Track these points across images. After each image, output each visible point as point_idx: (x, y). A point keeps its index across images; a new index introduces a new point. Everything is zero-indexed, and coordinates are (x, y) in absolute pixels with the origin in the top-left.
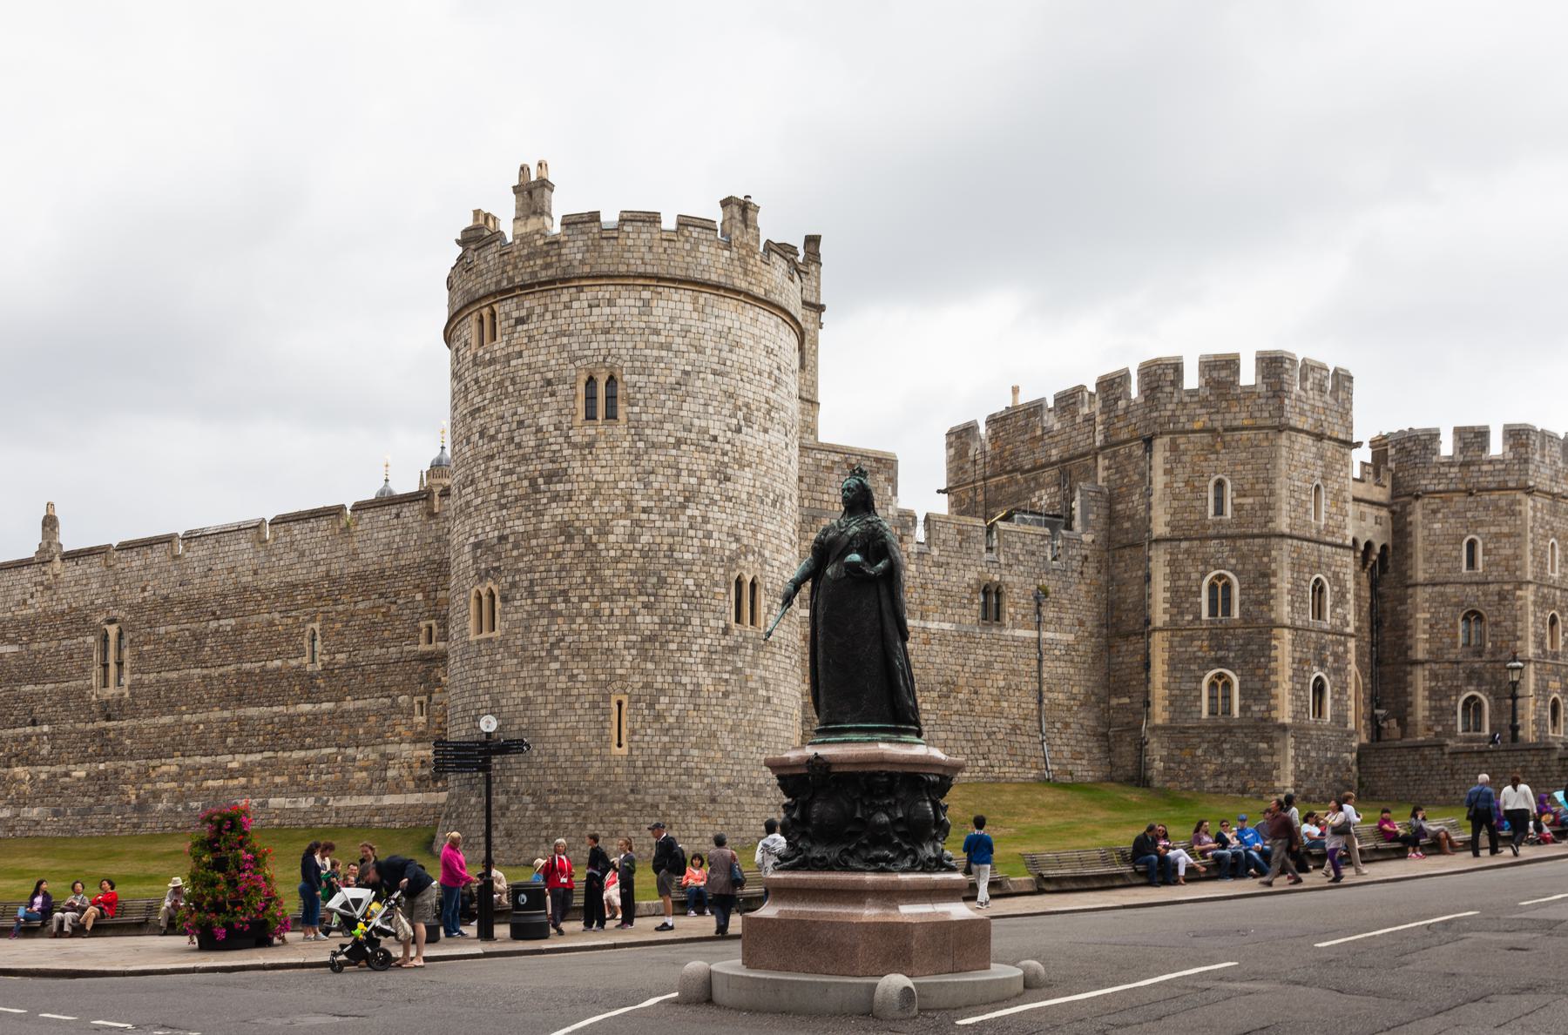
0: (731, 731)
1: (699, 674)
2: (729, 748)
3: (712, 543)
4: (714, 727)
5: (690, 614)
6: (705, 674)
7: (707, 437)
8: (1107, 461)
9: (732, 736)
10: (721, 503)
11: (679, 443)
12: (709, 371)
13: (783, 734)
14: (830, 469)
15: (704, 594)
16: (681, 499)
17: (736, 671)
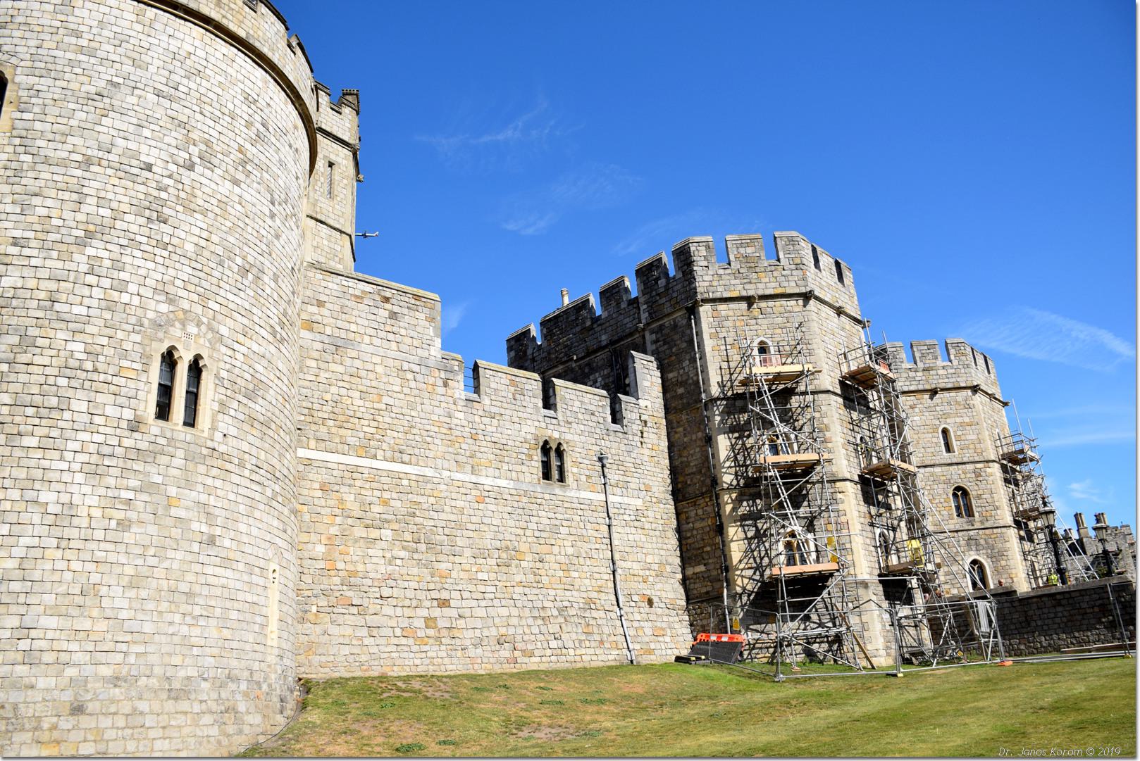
0: (131, 586)
1: (75, 489)
2: (124, 614)
3: (125, 298)
4: (95, 578)
5: (70, 393)
6: (87, 489)
7: (134, 163)
8: (654, 336)
9: (132, 593)
10: (149, 249)
11: (87, 162)
12: (151, 90)
13: (241, 596)
14: (359, 299)
15: (101, 367)
16: (82, 234)
17: (147, 487)
